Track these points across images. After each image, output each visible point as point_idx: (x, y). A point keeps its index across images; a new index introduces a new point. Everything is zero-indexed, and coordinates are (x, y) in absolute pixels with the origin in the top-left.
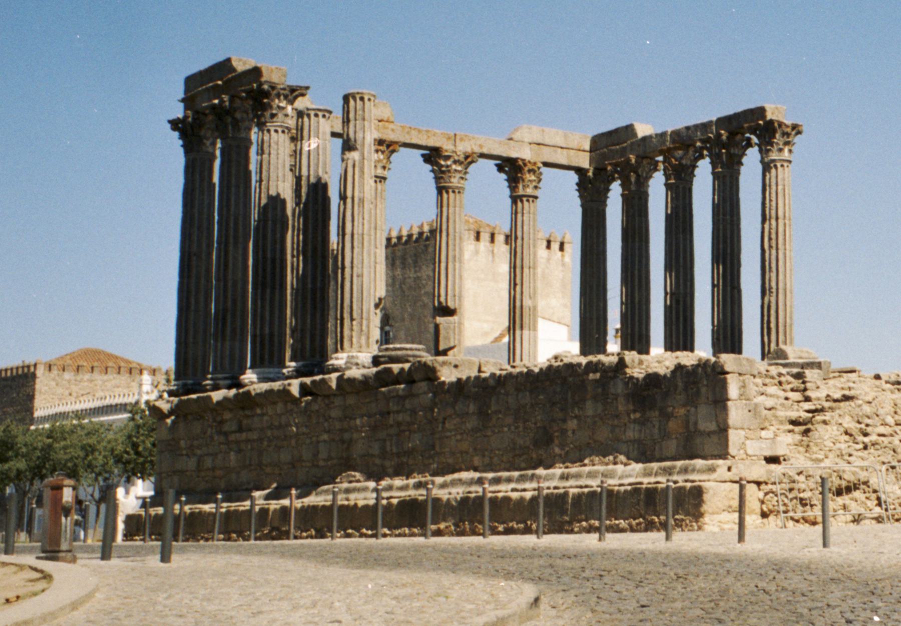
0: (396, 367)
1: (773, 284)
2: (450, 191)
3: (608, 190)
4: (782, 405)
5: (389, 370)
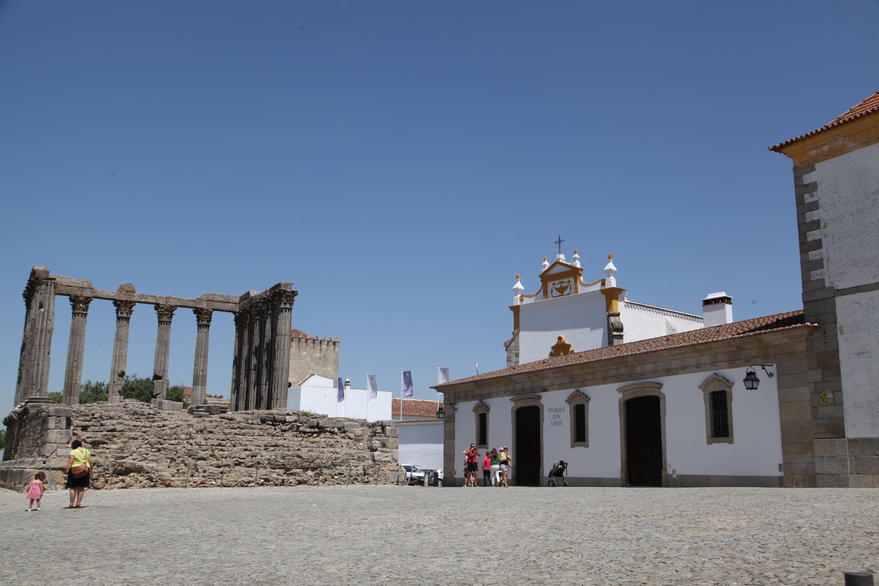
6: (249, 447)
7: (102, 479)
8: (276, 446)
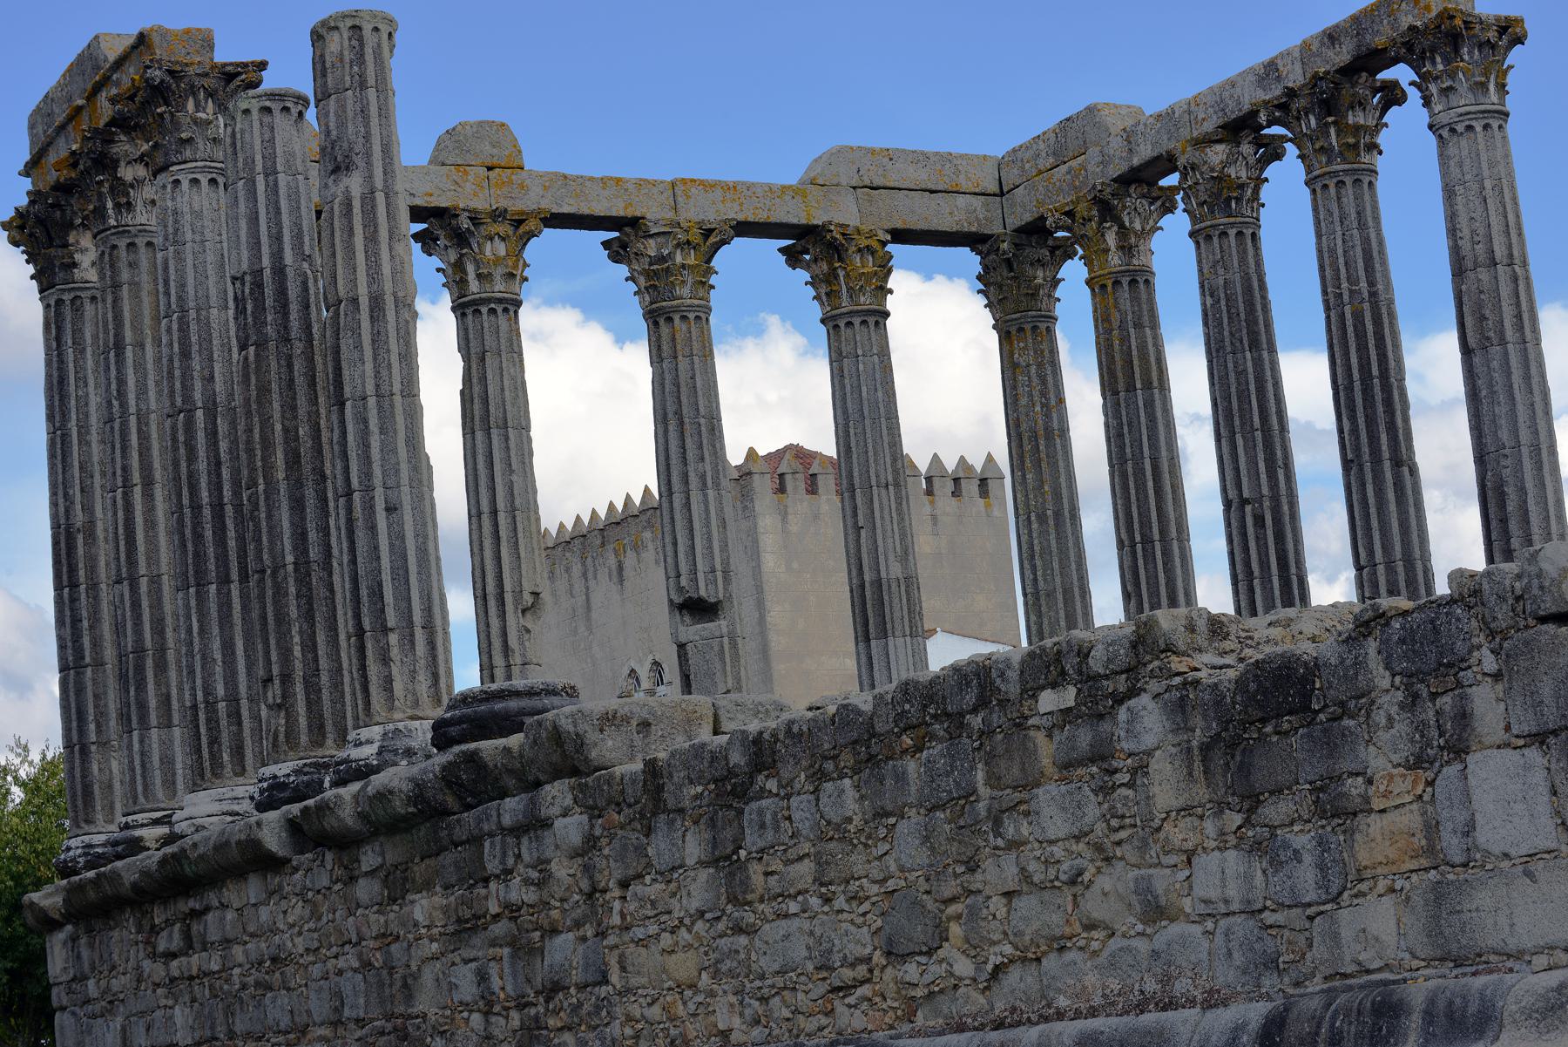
0: (488, 747)
1: (1504, 435)
2: (677, 318)
3: (1056, 283)
5: (472, 758)
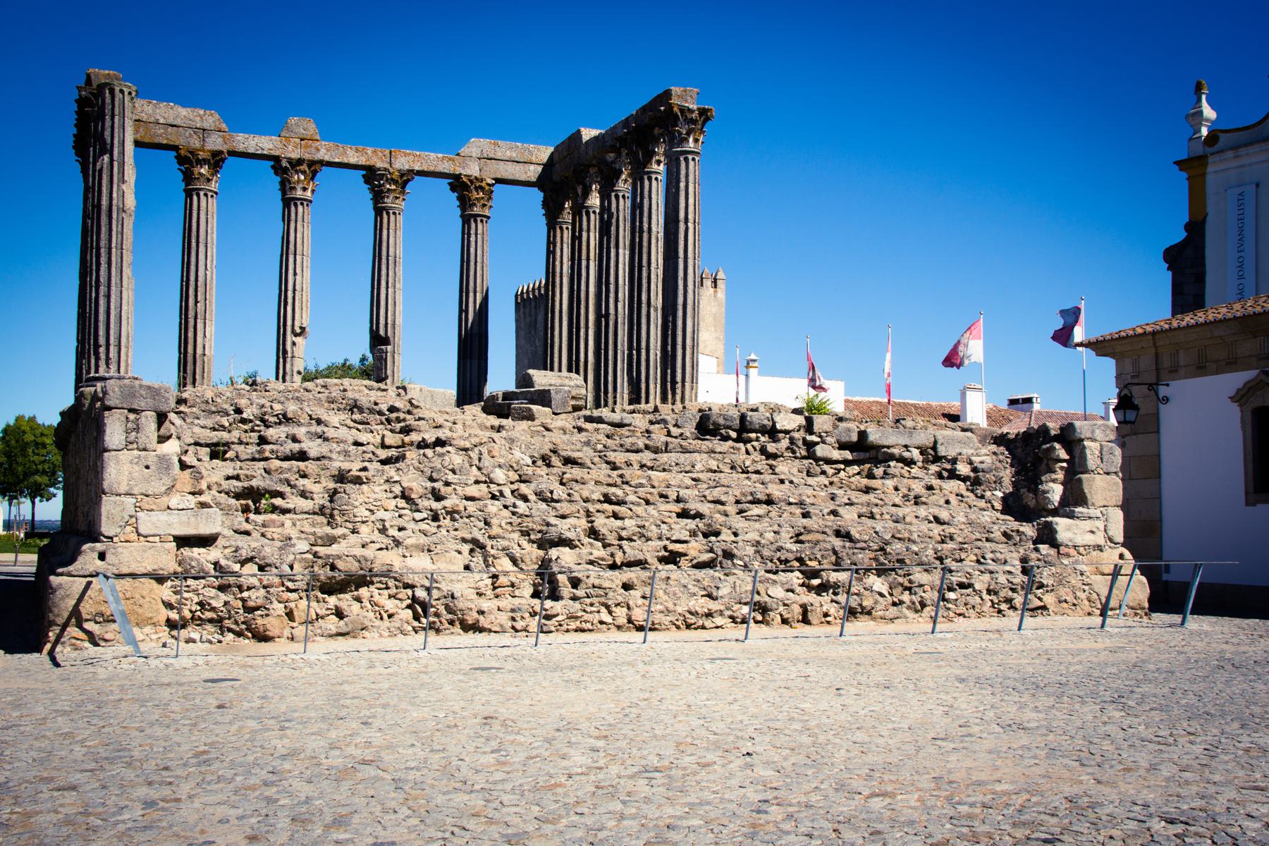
4: (346, 453)
6: (694, 506)
7: (279, 608)
8: (769, 502)
